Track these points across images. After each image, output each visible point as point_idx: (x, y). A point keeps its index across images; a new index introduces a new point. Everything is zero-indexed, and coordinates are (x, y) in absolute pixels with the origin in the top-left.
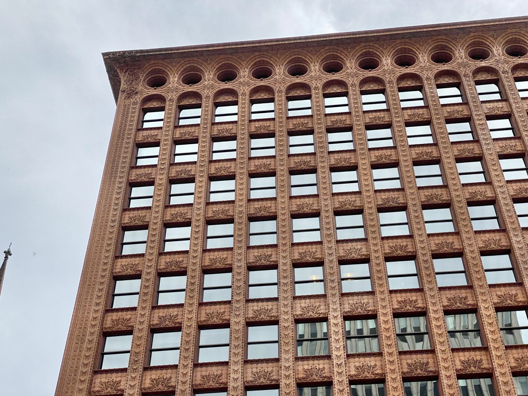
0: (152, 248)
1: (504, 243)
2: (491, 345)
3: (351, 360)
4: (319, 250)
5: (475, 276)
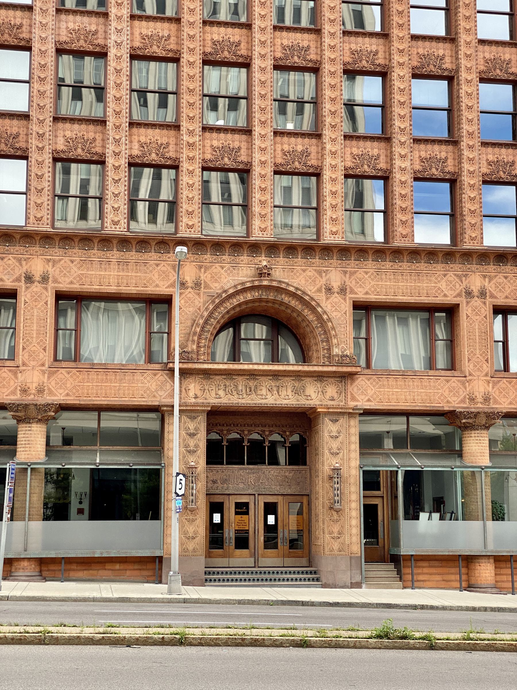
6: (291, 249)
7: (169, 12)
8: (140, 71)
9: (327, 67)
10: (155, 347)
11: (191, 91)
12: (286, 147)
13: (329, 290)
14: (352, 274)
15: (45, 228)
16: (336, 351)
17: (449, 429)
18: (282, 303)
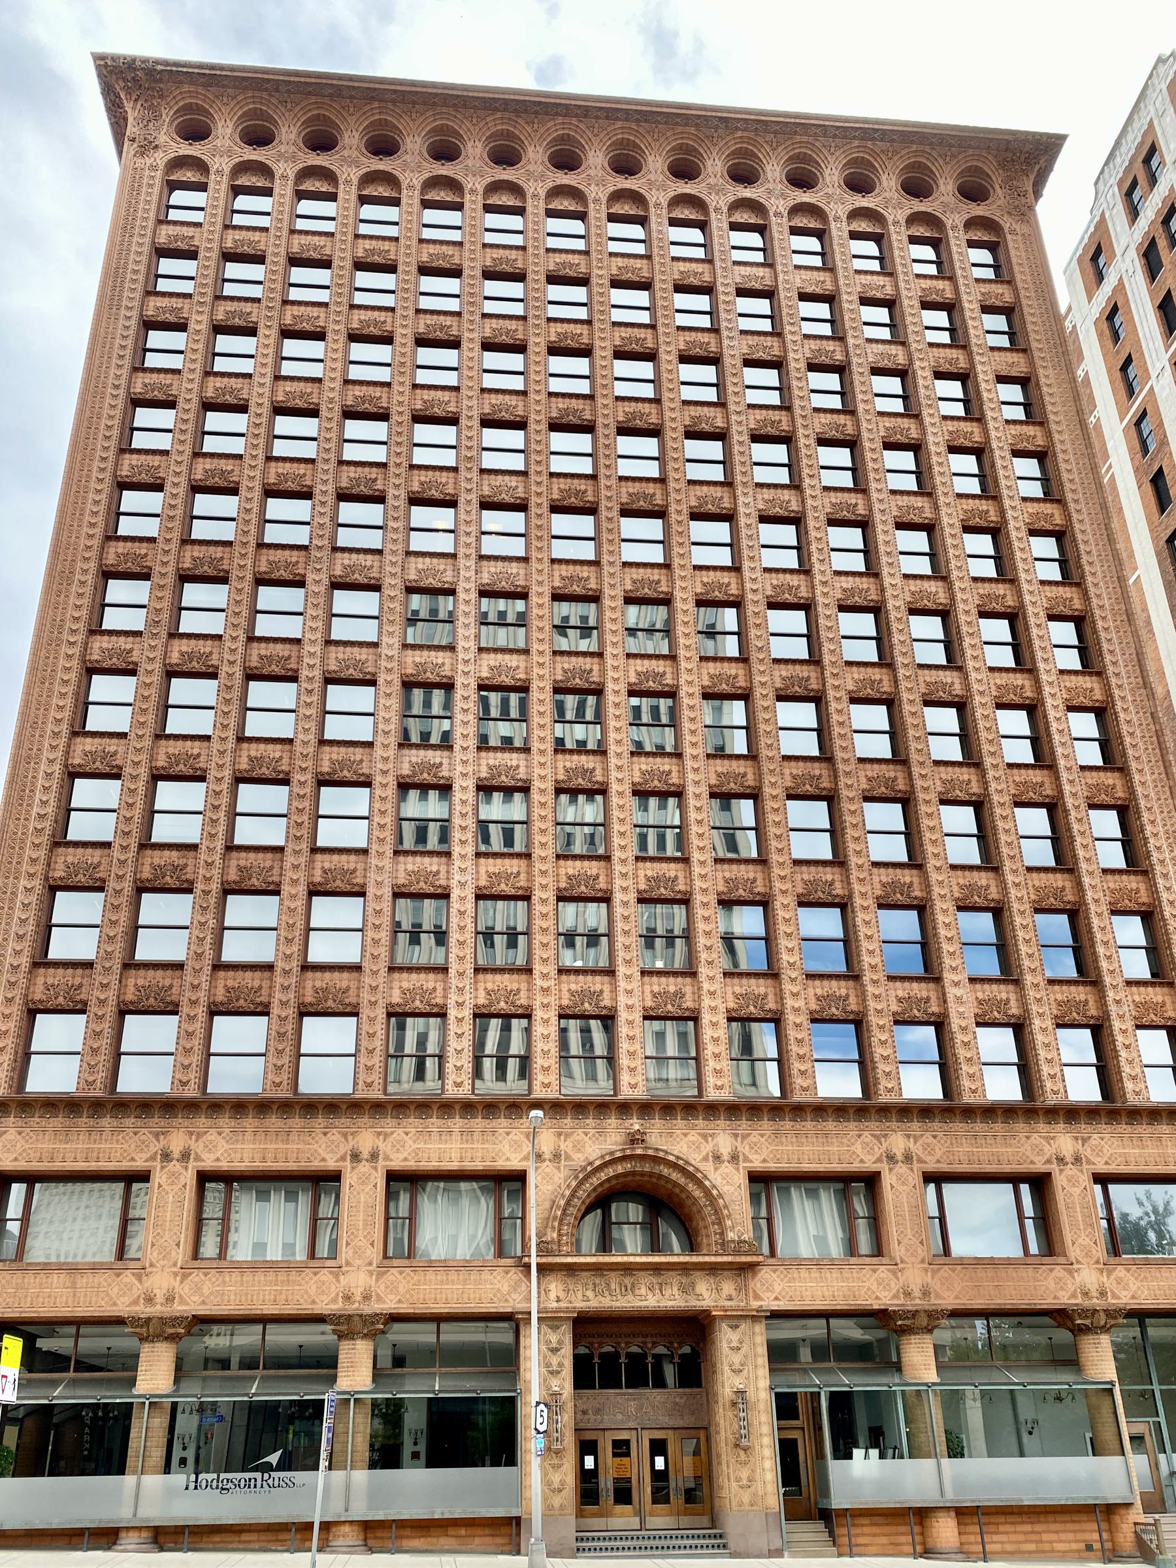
0: (182, 442)
1: (726, 504)
2: (682, 653)
3: (484, 656)
4: (451, 481)
5: (677, 550)
6: (668, 1109)
7: (518, 847)
8: (486, 910)
9: (698, 898)
10: (506, 1236)
11: (544, 930)
12: (656, 989)
13: (717, 1158)
14: (744, 1137)
15: (376, 1094)
16: (731, 1235)
17: (881, 1334)
18: (660, 1176)
